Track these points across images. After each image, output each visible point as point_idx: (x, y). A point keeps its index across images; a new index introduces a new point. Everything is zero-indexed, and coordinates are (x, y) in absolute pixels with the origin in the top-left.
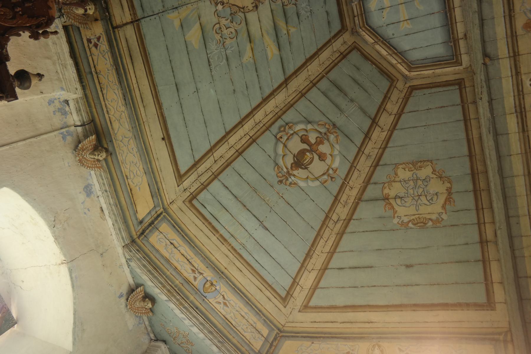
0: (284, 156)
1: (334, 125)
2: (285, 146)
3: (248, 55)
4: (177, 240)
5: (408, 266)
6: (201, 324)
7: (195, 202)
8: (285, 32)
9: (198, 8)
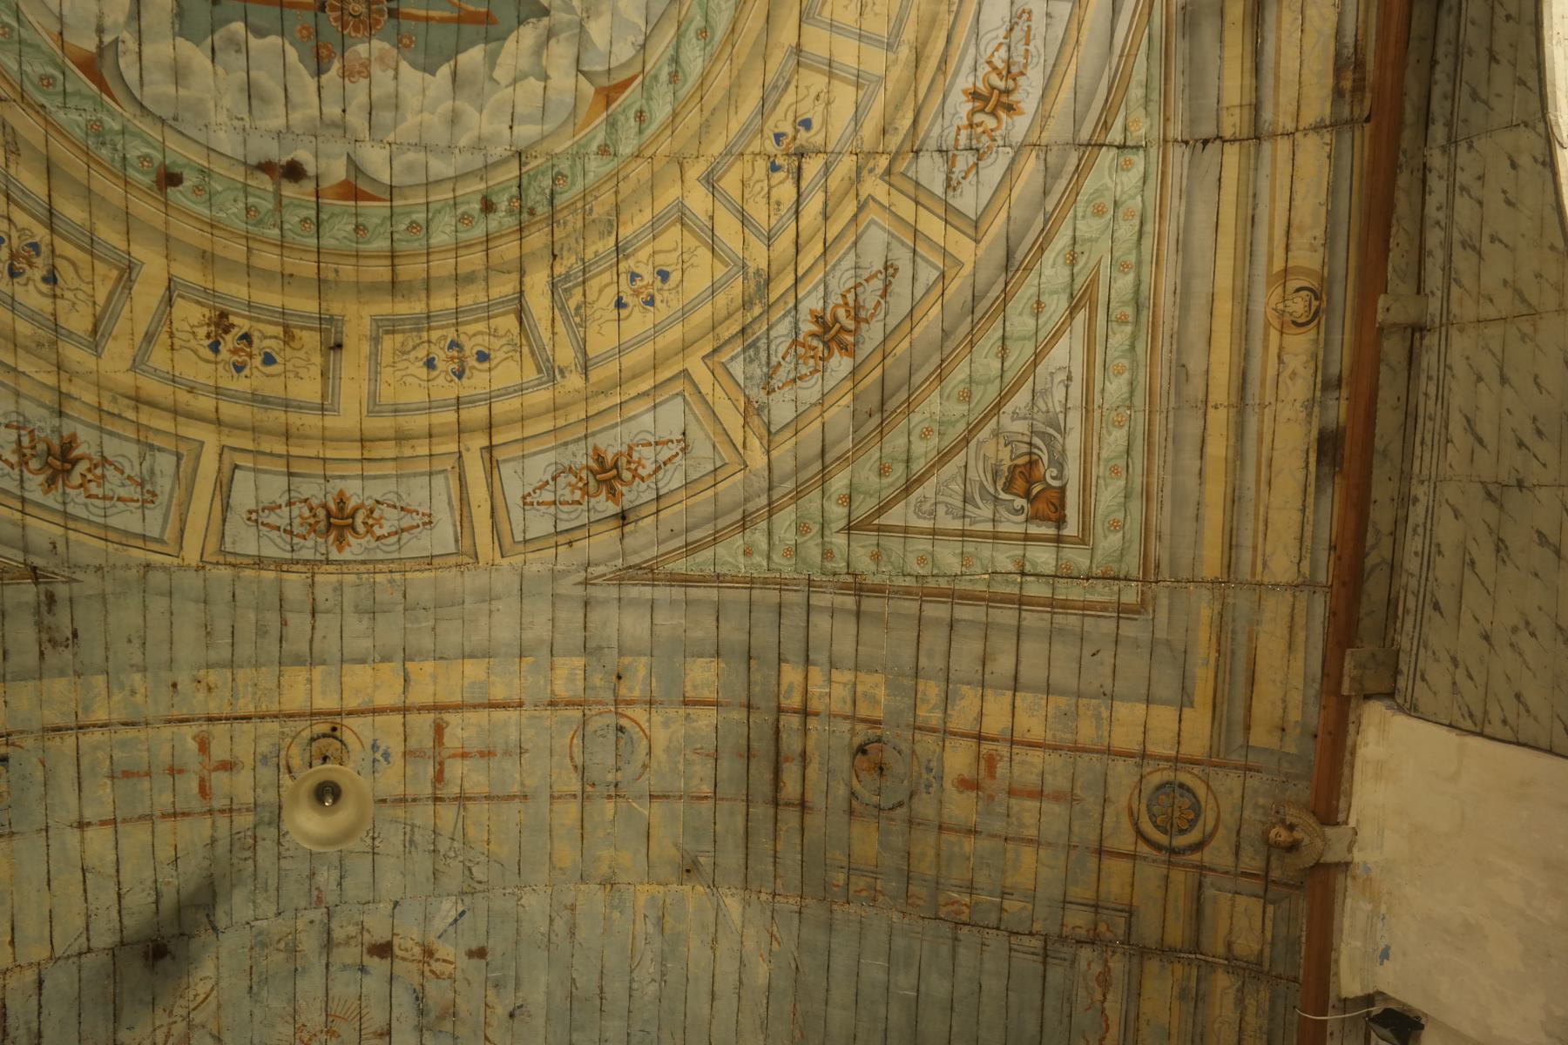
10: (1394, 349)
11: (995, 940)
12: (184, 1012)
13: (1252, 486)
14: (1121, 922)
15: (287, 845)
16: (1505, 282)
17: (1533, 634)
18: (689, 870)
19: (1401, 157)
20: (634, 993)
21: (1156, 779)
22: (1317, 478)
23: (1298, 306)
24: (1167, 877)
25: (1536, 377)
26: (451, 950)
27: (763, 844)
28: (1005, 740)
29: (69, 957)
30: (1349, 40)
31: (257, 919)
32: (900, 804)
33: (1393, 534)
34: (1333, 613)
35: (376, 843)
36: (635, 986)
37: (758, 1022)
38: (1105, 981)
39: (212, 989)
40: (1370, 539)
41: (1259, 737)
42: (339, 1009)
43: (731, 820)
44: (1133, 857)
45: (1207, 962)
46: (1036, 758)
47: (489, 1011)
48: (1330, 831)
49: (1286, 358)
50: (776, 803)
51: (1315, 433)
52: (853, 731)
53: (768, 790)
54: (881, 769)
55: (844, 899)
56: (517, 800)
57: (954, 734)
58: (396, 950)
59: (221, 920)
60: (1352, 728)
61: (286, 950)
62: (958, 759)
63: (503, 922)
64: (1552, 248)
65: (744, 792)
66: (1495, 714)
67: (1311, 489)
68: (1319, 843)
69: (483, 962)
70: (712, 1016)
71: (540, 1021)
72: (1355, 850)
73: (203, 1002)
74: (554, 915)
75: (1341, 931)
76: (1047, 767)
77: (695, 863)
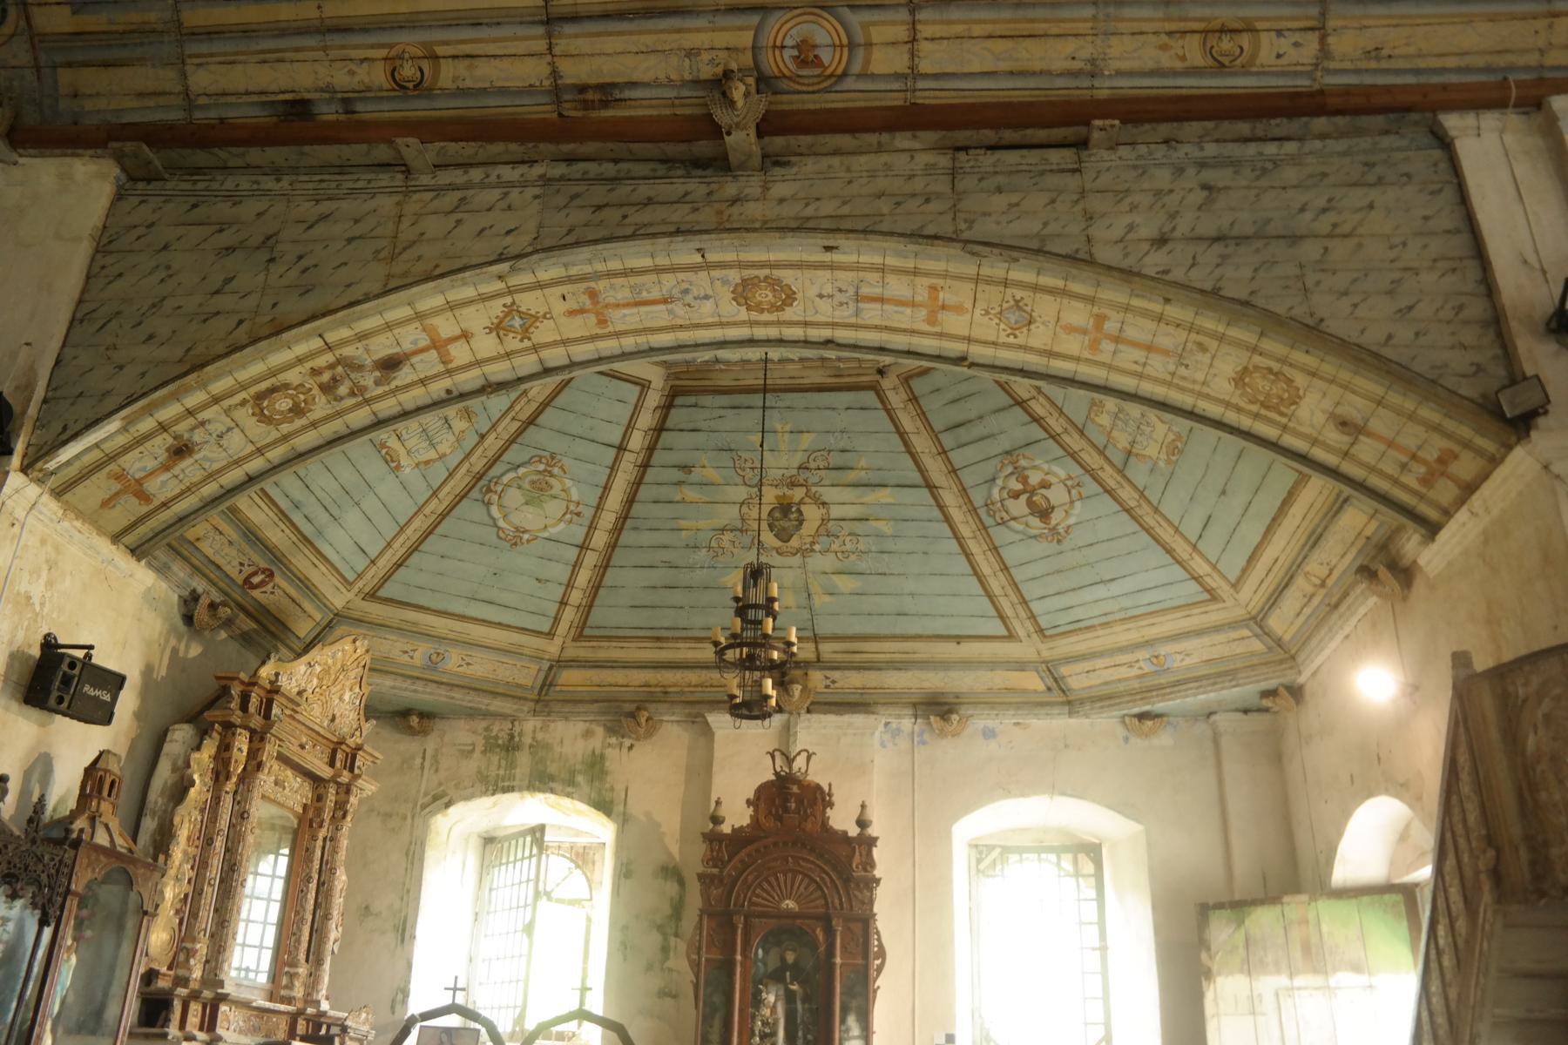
0: (1027, 525)
1: (1007, 453)
2: (1014, 519)
3: (885, 528)
4: (1087, 665)
5: (1224, 492)
6: (1198, 688)
7: (1047, 633)
8: (863, 472)
9: (814, 573)
10: (382, 152)
13: (259, 48)
16: (423, 234)
17: (162, 280)
19: (531, 145)
22: (273, 102)
23: (408, 71)
25: (346, 264)
30: (627, 94)
33: (248, 166)
34: (171, 127)
40: (234, 150)
49: (365, 65)
51: (307, 96)
60: (91, 152)
64: (437, 266)
66: (109, 260)
67: (264, 98)
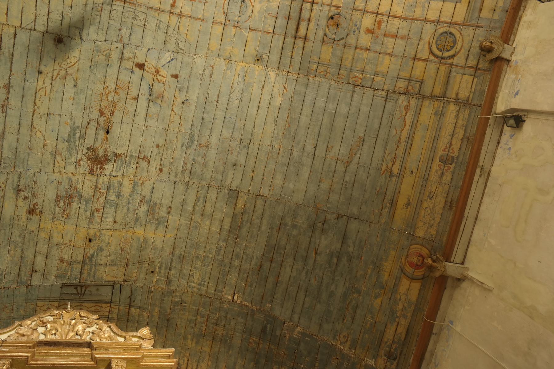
11: (369, 92)
12: (65, 67)
14: (418, 86)
15: (113, 15)
18: (259, 59)
20: (229, 103)
21: (441, 30)
24: (439, 68)
26: (166, 73)
27: (288, 52)
28: (387, 15)
29: (27, 29)
31: (97, 40)
32: (342, 39)
35: (146, 24)
36: (230, 100)
37: (273, 120)
38: (407, 108)
39: (77, 62)
41: (485, 14)
42: (121, 84)
43: (278, 42)
44: (427, 61)
45: (447, 101)
46: (397, 22)
47: (175, 99)
48: (506, 45)
50: (295, 37)
52: (329, 10)
53: (293, 32)
54: (338, 25)
55: (314, 75)
56: (200, 20)
57: (368, 12)
58: (146, 67)
59: (84, 37)
61: (106, 56)
62: (368, 21)
63: (186, 66)
65: (284, 32)
68: (501, 48)
69: (176, 80)
70: (257, 115)
71: (193, 107)
72: (513, 56)
73: (73, 66)
74: (205, 68)
75: (501, 87)
76: (400, 26)
77: (261, 57)
